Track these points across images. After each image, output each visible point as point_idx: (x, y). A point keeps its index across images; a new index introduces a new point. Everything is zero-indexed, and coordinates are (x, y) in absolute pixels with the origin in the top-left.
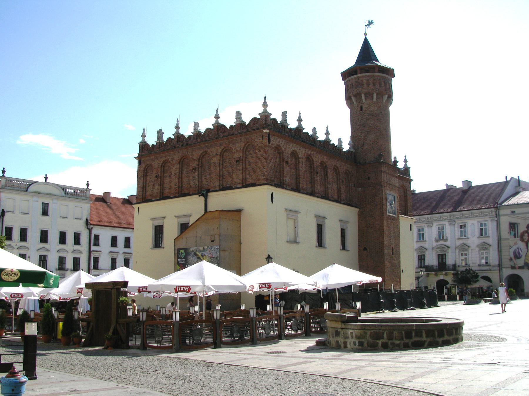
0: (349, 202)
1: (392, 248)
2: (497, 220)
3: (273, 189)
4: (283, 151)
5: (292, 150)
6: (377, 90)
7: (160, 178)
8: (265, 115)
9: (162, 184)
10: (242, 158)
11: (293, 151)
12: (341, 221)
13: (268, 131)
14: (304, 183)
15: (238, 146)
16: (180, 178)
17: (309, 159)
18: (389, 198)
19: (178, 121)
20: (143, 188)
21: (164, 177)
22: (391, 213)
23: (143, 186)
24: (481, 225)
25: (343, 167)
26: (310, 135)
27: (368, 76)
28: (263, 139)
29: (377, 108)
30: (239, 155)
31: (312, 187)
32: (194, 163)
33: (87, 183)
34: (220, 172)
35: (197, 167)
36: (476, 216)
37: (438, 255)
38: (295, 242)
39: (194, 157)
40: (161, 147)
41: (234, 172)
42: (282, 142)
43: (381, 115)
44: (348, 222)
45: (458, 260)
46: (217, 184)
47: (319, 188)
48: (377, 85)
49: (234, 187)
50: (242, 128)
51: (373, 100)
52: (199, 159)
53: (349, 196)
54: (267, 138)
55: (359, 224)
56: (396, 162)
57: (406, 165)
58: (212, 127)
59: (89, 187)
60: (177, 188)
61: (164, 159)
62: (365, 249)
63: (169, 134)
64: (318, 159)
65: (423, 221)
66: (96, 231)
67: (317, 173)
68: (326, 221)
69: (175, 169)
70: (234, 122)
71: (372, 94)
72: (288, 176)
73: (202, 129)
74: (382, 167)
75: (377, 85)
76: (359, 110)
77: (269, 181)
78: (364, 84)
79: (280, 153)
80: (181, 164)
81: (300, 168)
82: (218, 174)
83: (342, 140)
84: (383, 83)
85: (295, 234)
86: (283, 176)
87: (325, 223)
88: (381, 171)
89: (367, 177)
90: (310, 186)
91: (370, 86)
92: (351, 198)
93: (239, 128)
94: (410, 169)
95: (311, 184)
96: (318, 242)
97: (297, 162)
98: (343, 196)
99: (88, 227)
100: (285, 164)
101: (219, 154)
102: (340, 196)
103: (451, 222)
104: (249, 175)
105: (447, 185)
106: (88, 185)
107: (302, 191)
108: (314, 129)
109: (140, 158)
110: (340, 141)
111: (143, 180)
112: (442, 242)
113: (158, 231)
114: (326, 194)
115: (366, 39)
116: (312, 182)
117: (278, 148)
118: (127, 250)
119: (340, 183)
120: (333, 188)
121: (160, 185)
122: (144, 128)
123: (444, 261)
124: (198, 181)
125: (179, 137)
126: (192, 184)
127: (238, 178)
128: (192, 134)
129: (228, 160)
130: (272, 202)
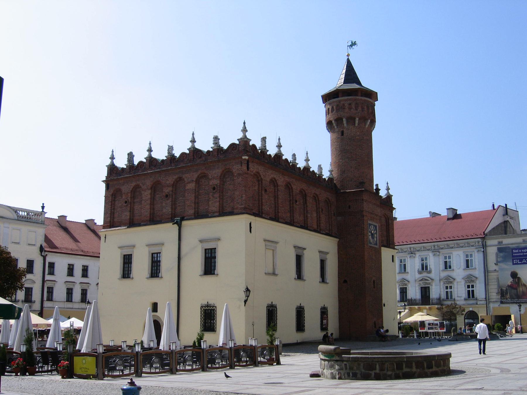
0: (328, 232)
1: (374, 280)
2: (484, 251)
3: (251, 218)
4: (261, 179)
5: (270, 177)
6: (359, 114)
7: (131, 204)
8: (245, 141)
9: (132, 211)
10: (220, 185)
11: (272, 178)
12: (320, 252)
13: (247, 158)
15: (215, 172)
16: (152, 204)
17: (288, 187)
18: (370, 229)
19: (150, 144)
20: (111, 214)
21: (134, 203)
22: (373, 243)
23: (111, 212)
24: (467, 256)
25: (324, 195)
26: (289, 162)
27: (350, 100)
28: (241, 166)
29: (358, 133)
30: (216, 182)
31: (291, 216)
32: (167, 189)
33: (42, 205)
34: (195, 199)
35: (171, 193)
36: (462, 247)
37: (421, 288)
38: (274, 274)
39: (168, 182)
40: (131, 170)
41: (211, 199)
42: (261, 169)
43: (363, 141)
44: (328, 253)
45: (442, 293)
46: (191, 212)
47: (298, 217)
48: (360, 109)
49: (210, 215)
50: (219, 153)
51: (355, 125)
52: (173, 185)
53: (328, 225)
54: (246, 165)
56: (378, 190)
57: (388, 192)
58: (188, 152)
59: (44, 210)
60: (149, 215)
61: (133, 184)
62: (345, 281)
63: (140, 157)
64: (297, 186)
65: (406, 252)
66: (50, 258)
67: (296, 201)
68: (305, 252)
69: (146, 195)
70: (212, 148)
71: (355, 119)
72: (267, 205)
73: (177, 153)
74: (364, 196)
75: (360, 109)
76: (340, 135)
77: (248, 210)
78: (346, 107)
79: (258, 181)
80: (153, 188)
81: (279, 196)
82: (194, 201)
83: (322, 166)
84: (365, 107)
86: (262, 205)
87: (304, 254)
88: (363, 199)
90: (289, 215)
91: (352, 110)
92: (331, 228)
93: (216, 154)
94: (392, 197)
95: (290, 213)
96: (297, 274)
99: (43, 254)
100: (263, 192)
101: (194, 180)
102: (320, 226)
103: (435, 253)
104: (226, 203)
105: (430, 212)
106: (43, 207)
107: (280, 220)
108: (294, 155)
109: (108, 183)
110: (320, 167)
111: (111, 205)
112: (425, 274)
113: (127, 260)
114: (305, 223)
115: (348, 60)
116: (292, 211)
117: (257, 176)
118: (85, 280)
119: (319, 212)
120: (313, 216)
121: (130, 211)
122: (113, 150)
123: (428, 295)
124: (172, 208)
125: (151, 160)
126: (164, 211)
127: (214, 206)
128: (165, 158)
129: (204, 187)
130: (250, 231)
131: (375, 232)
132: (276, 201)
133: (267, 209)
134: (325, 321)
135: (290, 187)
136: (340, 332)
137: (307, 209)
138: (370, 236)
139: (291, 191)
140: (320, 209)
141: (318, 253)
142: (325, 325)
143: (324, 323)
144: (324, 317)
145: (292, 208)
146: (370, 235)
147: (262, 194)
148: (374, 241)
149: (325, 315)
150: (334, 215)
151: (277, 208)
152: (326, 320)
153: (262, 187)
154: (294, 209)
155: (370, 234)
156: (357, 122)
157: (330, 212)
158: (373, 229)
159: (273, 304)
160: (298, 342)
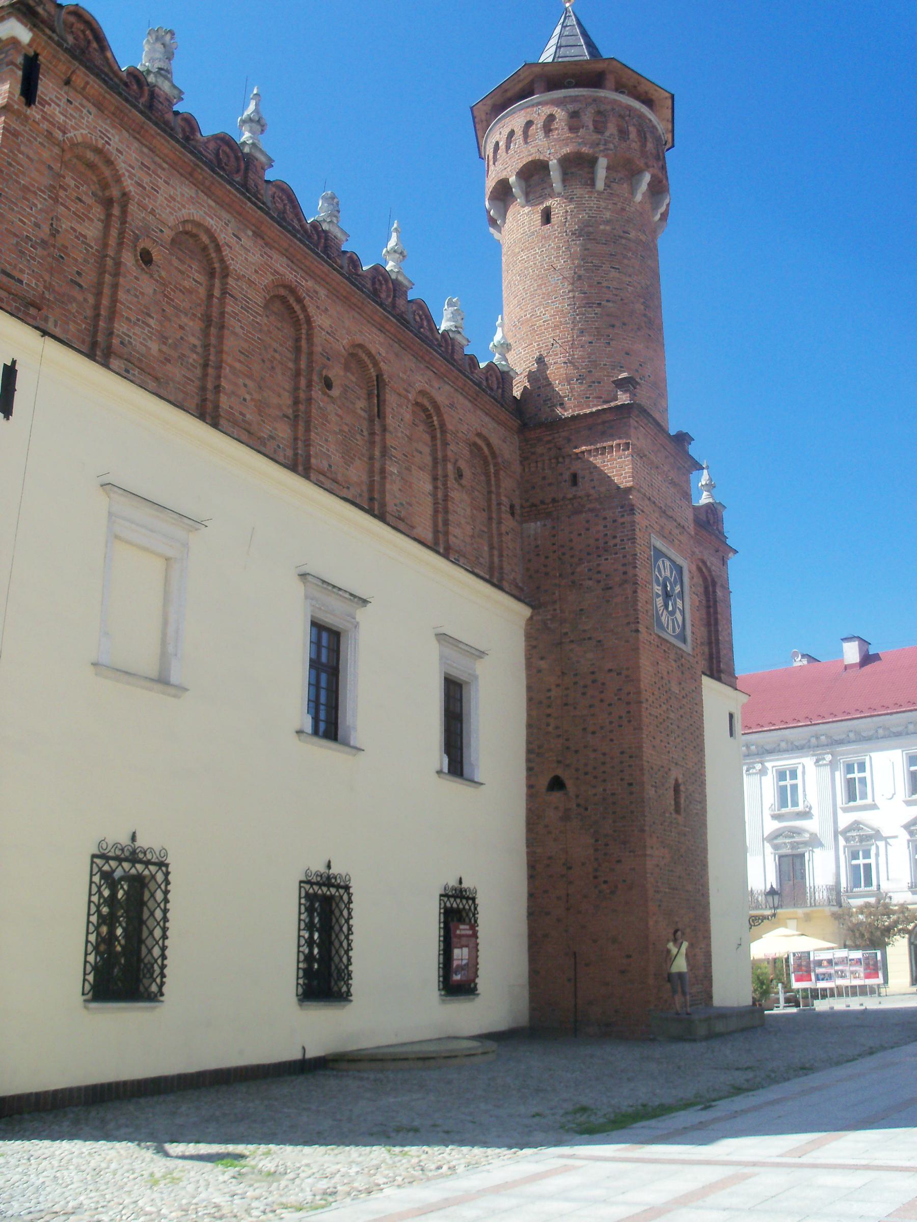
1: (676, 780)
5: (184, 213)
6: (611, 146)
14: (248, 397)
22: (670, 630)
31: (296, 439)
43: (624, 241)
44: (481, 654)
48: (612, 129)
51: (593, 184)
53: (486, 548)
55: (529, 677)
62: (557, 784)
68: (362, 615)
74: (632, 430)
76: (539, 222)
79: (108, 203)
81: (230, 321)
85: (164, 642)
87: (356, 626)
89: (567, 475)
92: (496, 560)
97: (217, 293)
98: (459, 534)
102: (446, 533)
119: (446, 476)
131: (678, 589)
132: (213, 340)
133: (149, 349)
134: (460, 955)
135: (302, 316)
136: (533, 998)
137: (384, 440)
138: (661, 598)
139: (304, 331)
140: (450, 467)
141: (434, 645)
142: (461, 968)
143: (455, 963)
144: (458, 932)
145: (302, 407)
146: (658, 596)
147: (118, 264)
148: (673, 620)
149: (462, 927)
150: (513, 514)
151: (211, 371)
152: (465, 950)
153: (122, 234)
154: (314, 411)
155: (658, 589)
156: (601, 173)
157: (494, 497)
158: (668, 574)
159: (138, 843)
160: (308, 1056)
